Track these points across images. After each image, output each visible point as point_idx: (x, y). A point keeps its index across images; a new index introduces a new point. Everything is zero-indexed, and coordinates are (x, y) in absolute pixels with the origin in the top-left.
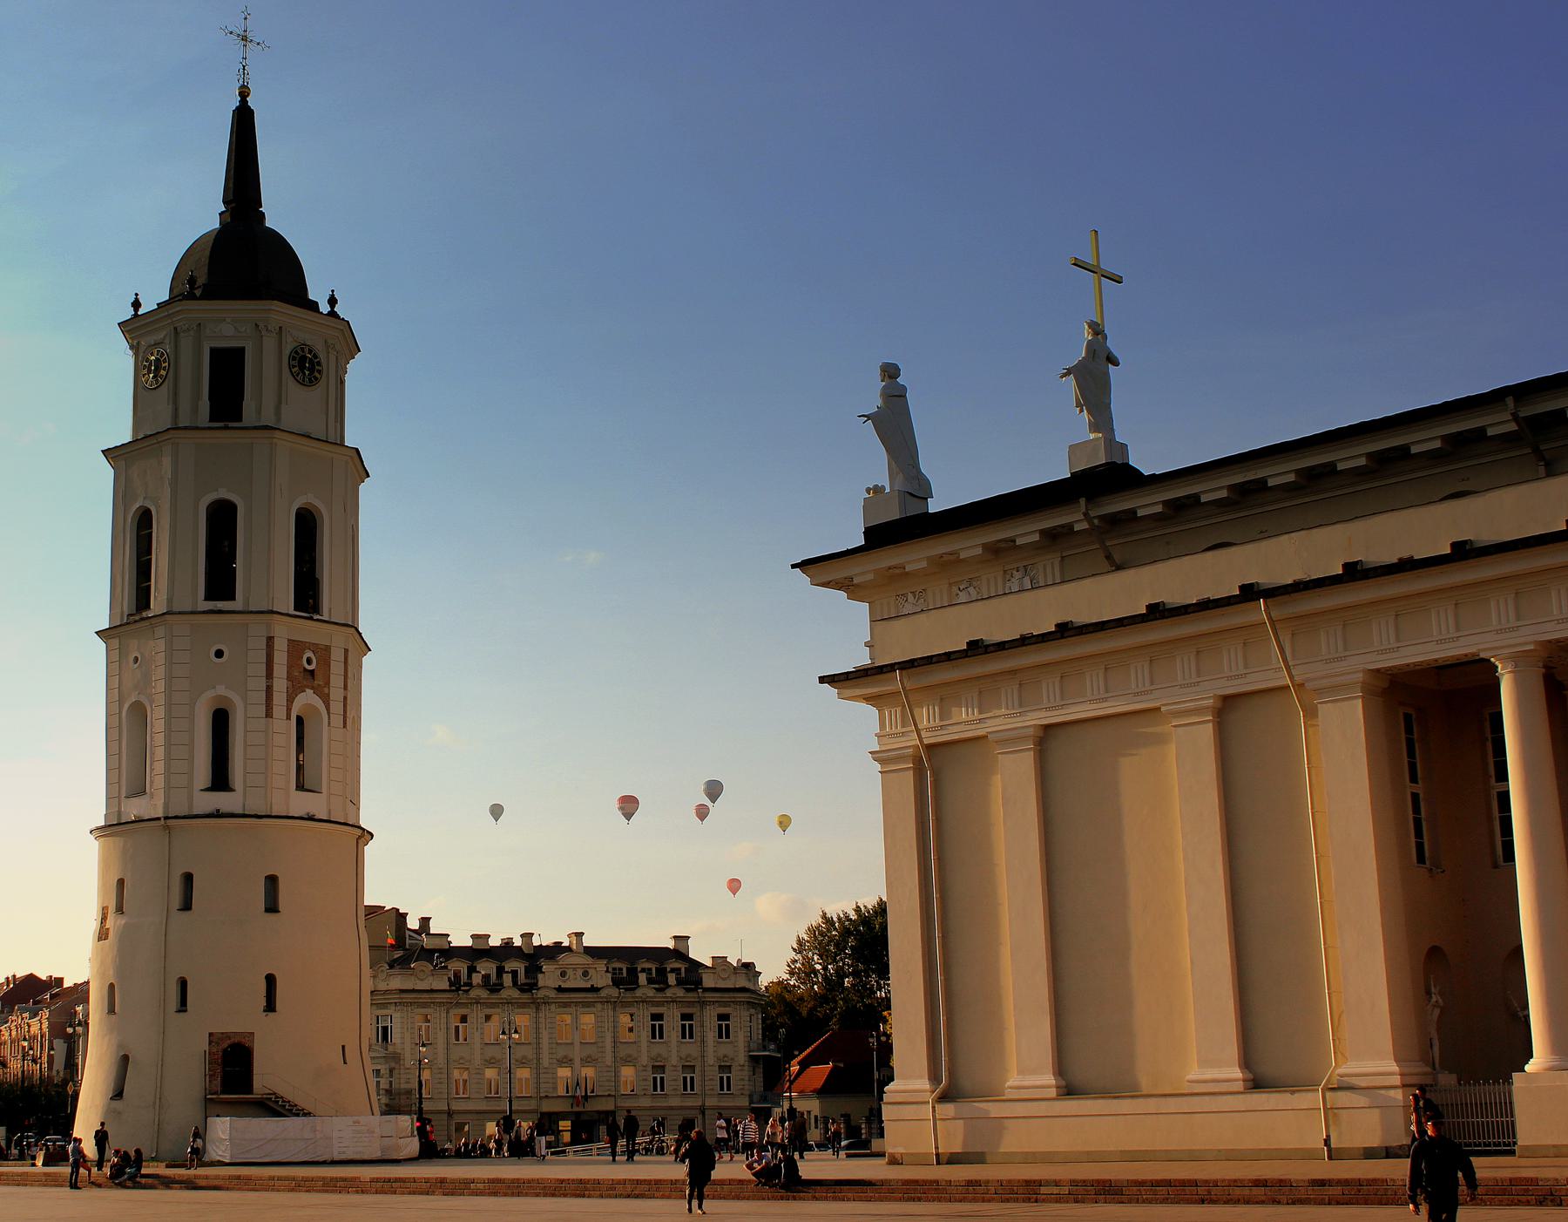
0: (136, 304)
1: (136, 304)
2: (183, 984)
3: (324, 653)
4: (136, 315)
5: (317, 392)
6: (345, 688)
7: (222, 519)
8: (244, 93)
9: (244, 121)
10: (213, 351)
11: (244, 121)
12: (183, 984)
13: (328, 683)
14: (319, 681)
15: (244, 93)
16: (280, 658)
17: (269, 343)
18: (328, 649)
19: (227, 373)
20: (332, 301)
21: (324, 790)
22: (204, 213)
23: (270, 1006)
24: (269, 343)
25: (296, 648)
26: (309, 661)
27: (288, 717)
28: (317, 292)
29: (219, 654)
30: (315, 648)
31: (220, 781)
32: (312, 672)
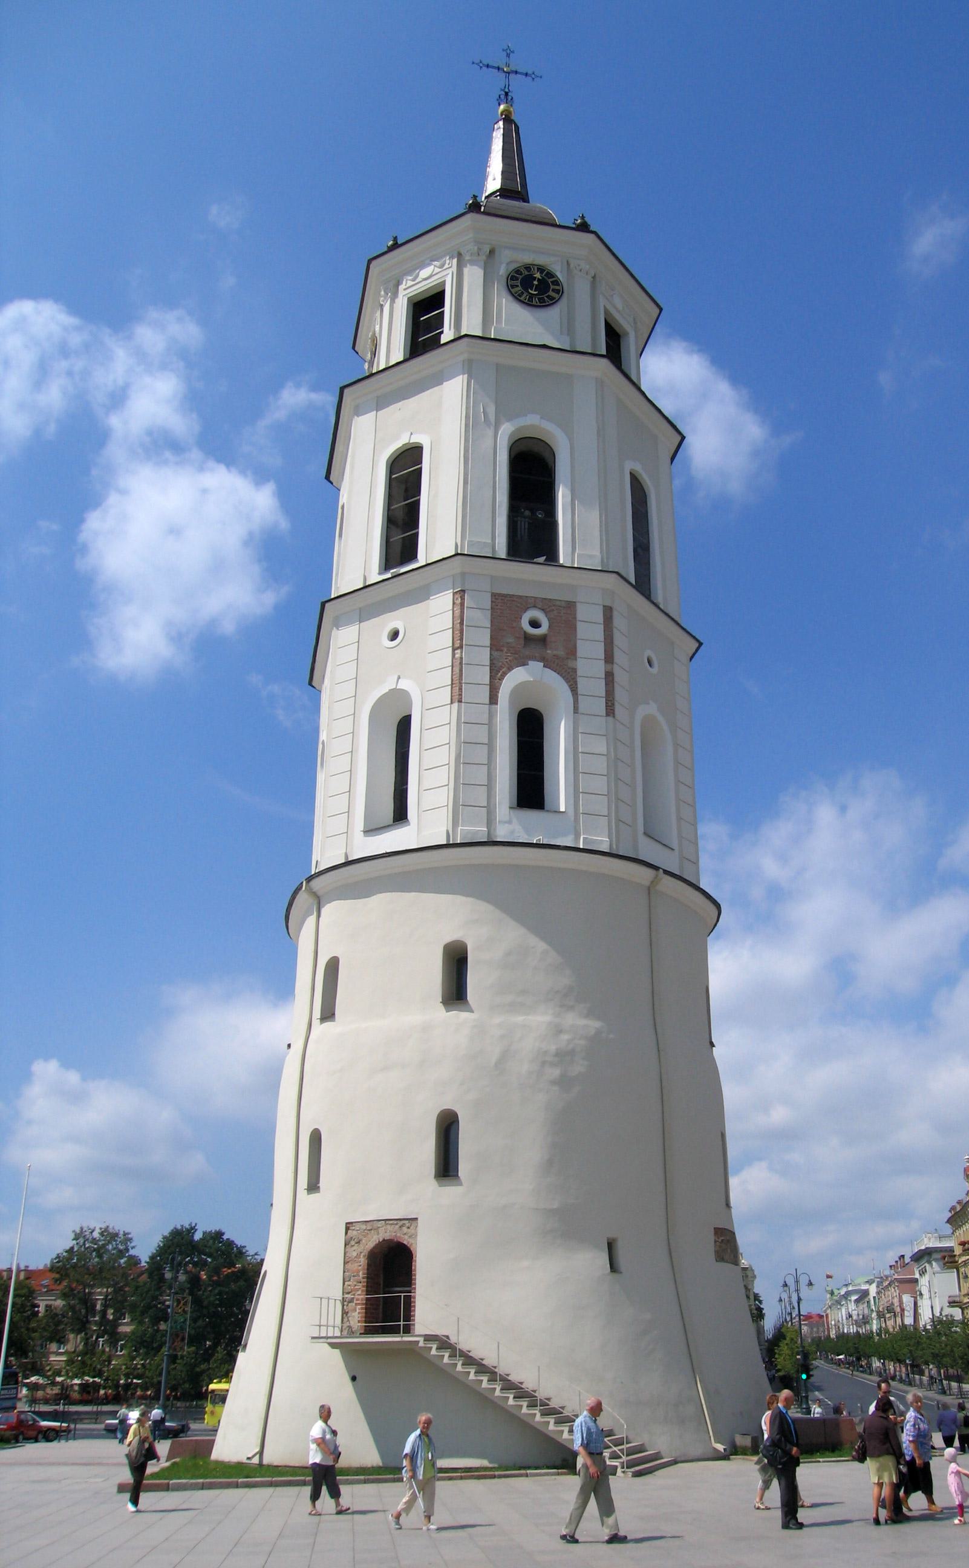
2: (316, 1138)
3: (564, 614)
6: (609, 658)
12: (316, 1138)
13: (572, 653)
14: (556, 650)
16: (480, 619)
18: (571, 606)
23: (446, 1166)
25: (505, 608)
26: (535, 624)
27: (493, 699)
29: (394, 635)
30: (546, 605)
31: (400, 815)
32: (543, 640)
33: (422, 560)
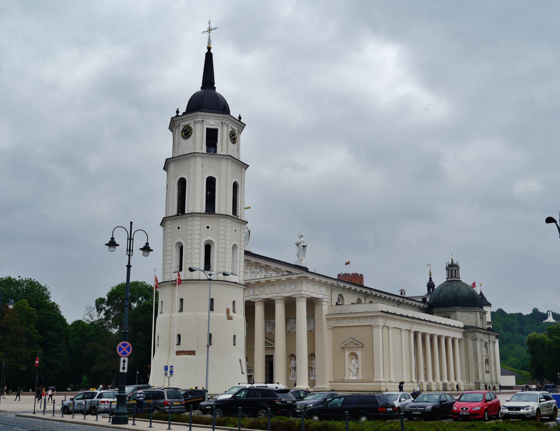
0: (178, 112)
1: (178, 112)
4: (177, 116)
5: (236, 145)
7: (211, 183)
8: (209, 48)
9: (209, 57)
10: (207, 129)
11: (209, 57)
15: (209, 48)
17: (225, 128)
19: (212, 137)
20: (240, 118)
21: (238, 274)
22: (196, 86)
24: (225, 128)
28: (234, 113)
33: (216, 212)
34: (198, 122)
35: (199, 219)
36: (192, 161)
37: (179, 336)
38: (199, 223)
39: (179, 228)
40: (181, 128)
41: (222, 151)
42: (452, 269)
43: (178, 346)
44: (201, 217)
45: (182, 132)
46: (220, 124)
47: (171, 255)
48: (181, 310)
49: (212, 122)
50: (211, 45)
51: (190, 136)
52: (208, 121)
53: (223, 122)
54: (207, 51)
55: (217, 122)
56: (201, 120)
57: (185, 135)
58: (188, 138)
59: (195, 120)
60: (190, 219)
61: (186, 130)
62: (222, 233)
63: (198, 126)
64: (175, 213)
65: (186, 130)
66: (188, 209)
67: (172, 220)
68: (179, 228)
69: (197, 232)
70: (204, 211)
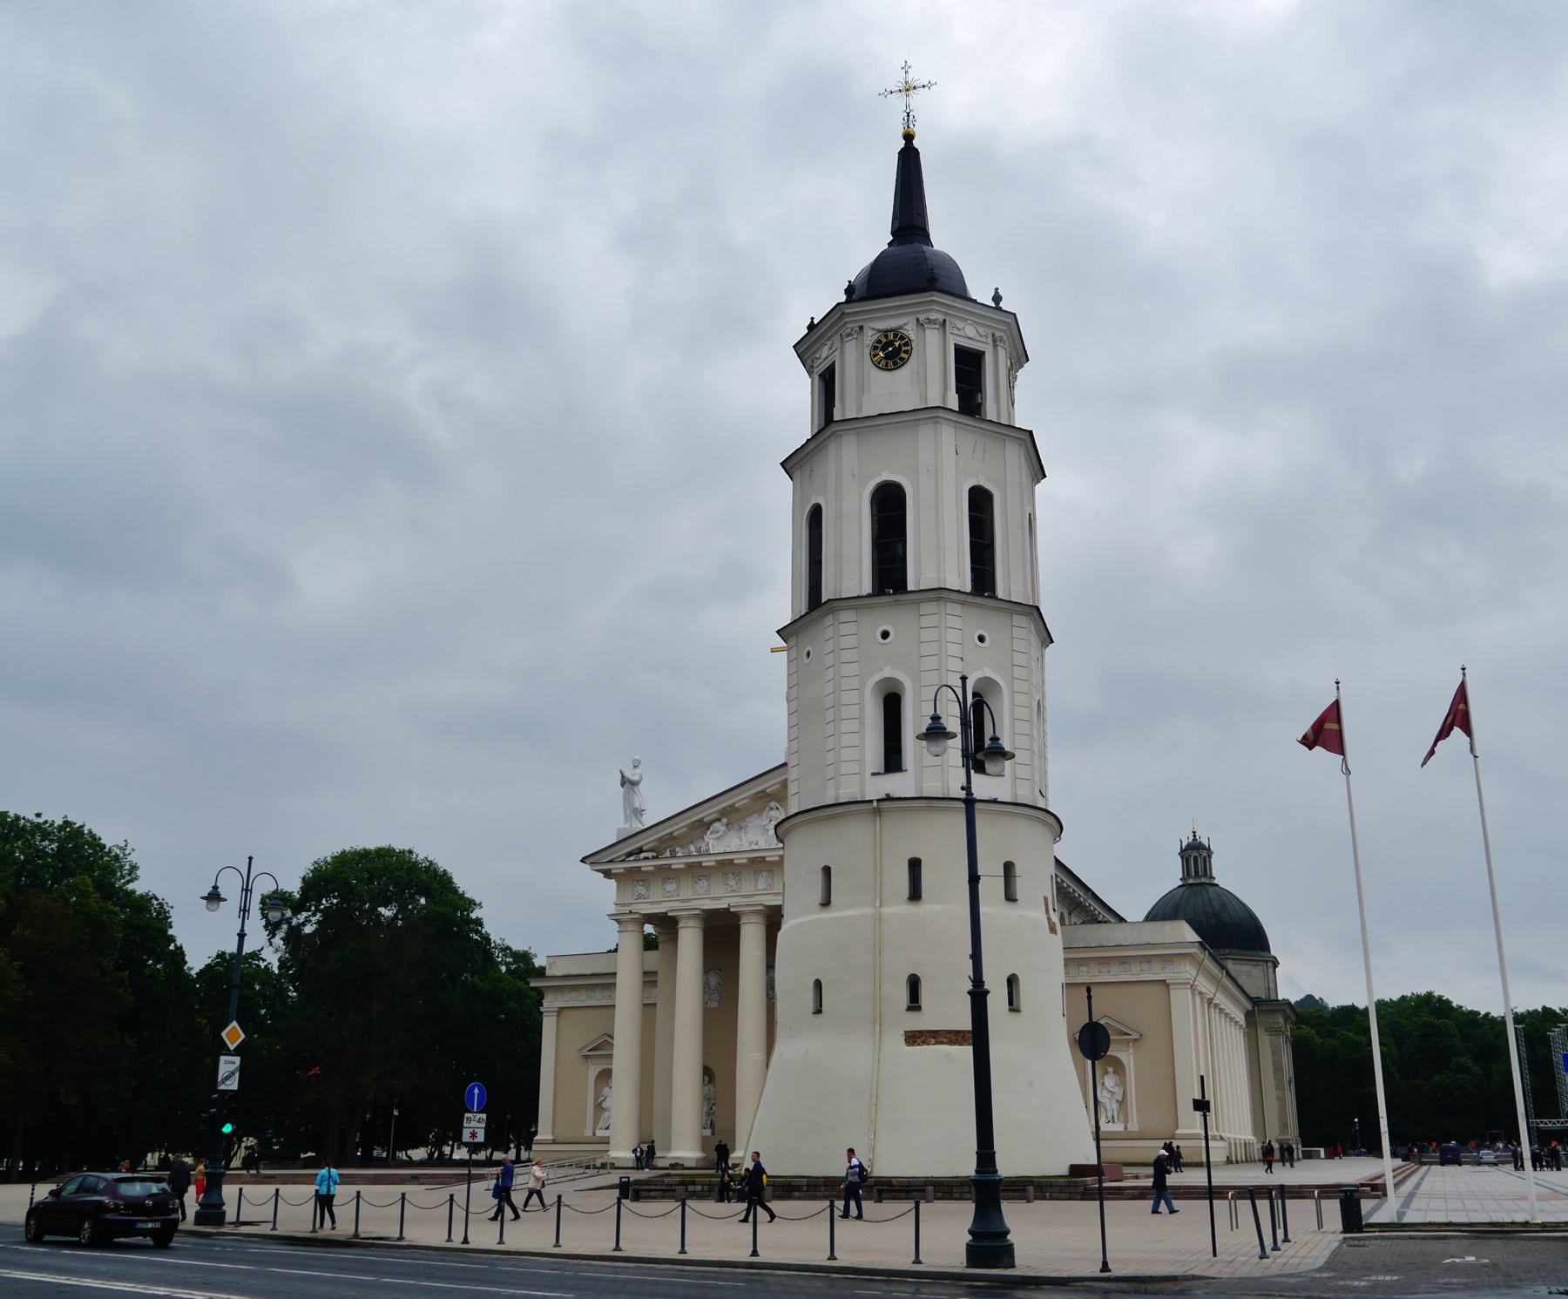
8: (909, 137)
9: (909, 161)
11: (909, 161)
15: (909, 137)
29: (981, 639)
33: (1000, 593)
34: (929, 321)
35: (957, 609)
36: (926, 433)
37: (914, 984)
38: (954, 622)
39: (885, 635)
40: (870, 337)
41: (999, 415)
42: (1195, 855)
43: (913, 1014)
44: (962, 603)
45: (875, 348)
46: (990, 340)
47: (861, 719)
48: (915, 894)
49: (970, 331)
50: (917, 130)
51: (904, 361)
52: (960, 324)
53: (998, 334)
54: (902, 144)
55: (982, 331)
56: (941, 318)
57: (888, 357)
58: (897, 367)
59: (922, 317)
60: (926, 608)
61: (891, 343)
62: (1019, 659)
63: (932, 335)
64: (867, 587)
65: (891, 343)
66: (918, 574)
67: (856, 608)
68: (885, 635)
69: (954, 650)
70: (968, 588)
